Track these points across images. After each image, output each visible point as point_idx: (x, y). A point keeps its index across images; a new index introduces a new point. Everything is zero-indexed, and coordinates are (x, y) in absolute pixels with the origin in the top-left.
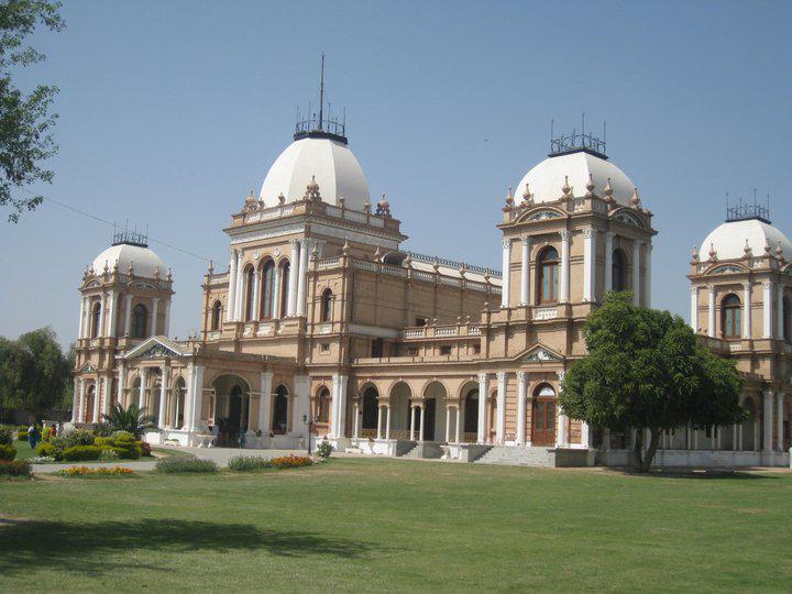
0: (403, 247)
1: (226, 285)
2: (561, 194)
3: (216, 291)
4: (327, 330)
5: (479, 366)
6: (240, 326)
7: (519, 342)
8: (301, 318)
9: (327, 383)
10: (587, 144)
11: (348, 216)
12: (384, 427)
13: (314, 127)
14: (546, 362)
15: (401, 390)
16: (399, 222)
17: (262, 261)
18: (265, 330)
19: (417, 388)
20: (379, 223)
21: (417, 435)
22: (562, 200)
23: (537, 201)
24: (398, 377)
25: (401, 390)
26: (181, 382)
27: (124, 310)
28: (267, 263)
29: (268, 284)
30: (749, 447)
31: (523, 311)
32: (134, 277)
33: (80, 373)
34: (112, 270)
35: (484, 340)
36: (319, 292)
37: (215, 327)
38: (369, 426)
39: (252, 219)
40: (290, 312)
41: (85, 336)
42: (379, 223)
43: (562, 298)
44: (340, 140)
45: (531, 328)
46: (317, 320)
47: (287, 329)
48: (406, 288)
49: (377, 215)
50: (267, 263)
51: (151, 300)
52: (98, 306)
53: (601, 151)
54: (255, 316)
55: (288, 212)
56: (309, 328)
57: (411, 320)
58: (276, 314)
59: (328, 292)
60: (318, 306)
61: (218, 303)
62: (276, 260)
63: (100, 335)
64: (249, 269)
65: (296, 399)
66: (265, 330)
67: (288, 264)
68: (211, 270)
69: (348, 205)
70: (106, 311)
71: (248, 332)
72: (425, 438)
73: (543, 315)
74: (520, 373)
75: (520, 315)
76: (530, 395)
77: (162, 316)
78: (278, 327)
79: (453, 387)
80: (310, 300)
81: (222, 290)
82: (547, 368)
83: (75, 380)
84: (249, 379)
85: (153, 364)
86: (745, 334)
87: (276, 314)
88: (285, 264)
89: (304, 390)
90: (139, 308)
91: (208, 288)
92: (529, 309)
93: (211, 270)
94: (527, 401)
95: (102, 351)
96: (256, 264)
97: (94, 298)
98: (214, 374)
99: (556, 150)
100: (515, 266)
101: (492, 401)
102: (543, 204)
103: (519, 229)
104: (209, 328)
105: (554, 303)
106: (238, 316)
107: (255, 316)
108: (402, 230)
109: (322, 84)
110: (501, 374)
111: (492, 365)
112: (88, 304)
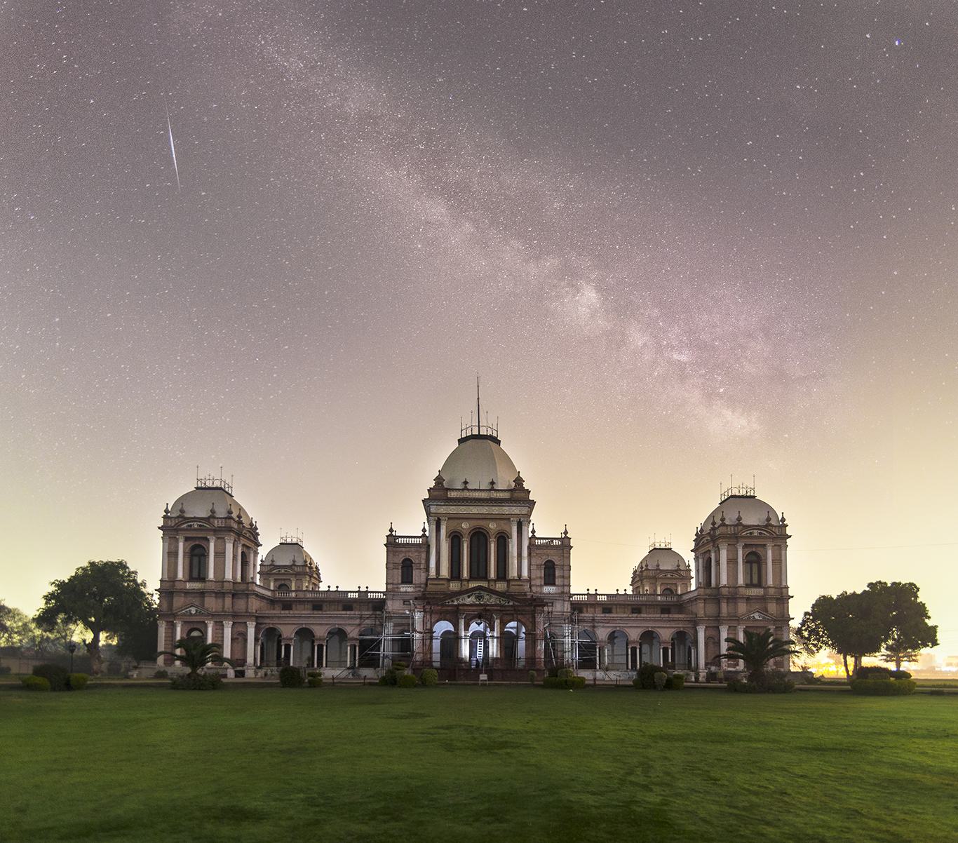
14: (761, 620)
37: (407, 579)
39: (452, 495)
47: (517, 587)
54: (465, 574)
55: (506, 495)
58: (492, 575)
62: (493, 532)
63: (211, 576)
64: (455, 539)
68: (391, 530)
71: (454, 586)
87: (492, 575)
88: (503, 540)
95: (220, 594)
100: (732, 561)
105: (759, 585)
106: (445, 572)
107: (465, 574)
109: (478, 399)
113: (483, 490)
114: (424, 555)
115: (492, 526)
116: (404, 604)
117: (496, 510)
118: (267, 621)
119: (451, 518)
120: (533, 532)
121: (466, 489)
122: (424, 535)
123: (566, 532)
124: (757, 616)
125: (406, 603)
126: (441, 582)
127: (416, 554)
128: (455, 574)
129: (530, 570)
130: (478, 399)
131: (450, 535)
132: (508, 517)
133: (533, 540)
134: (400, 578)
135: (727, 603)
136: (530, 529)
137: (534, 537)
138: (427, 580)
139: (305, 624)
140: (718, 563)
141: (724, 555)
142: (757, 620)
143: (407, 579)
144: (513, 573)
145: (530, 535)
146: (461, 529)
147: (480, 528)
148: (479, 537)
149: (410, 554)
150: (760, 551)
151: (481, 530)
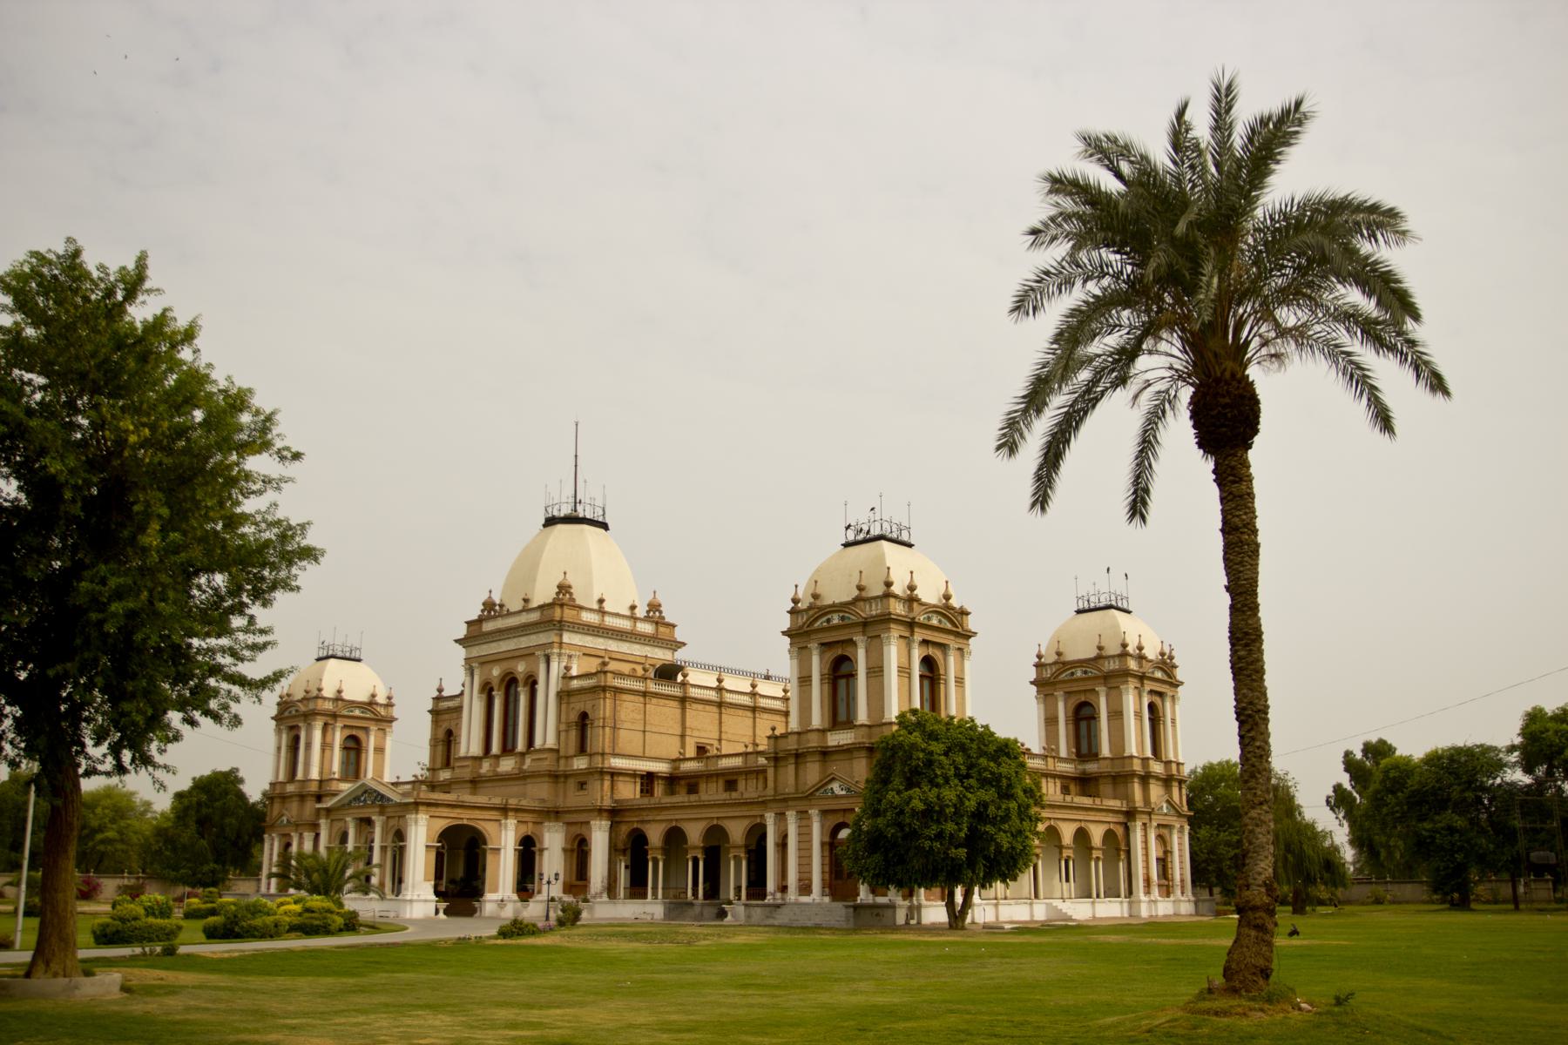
0: (680, 656)
1: (459, 709)
2: (856, 593)
4: (580, 763)
5: (764, 803)
6: (477, 760)
7: (812, 773)
8: (551, 750)
9: (583, 831)
10: (886, 531)
11: (610, 622)
12: (655, 888)
13: (566, 510)
14: (842, 797)
15: (675, 837)
16: (674, 626)
17: (502, 680)
18: (507, 765)
19: (695, 833)
20: (646, 628)
21: (695, 894)
22: (857, 600)
23: (828, 601)
25: (675, 837)
26: (400, 836)
27: (332, 747)
28: (510, 682)
29: (511, 707)
30: (1112, 892)
31: (793, 738)
32: (338, 699)
33: (272, 826)
34: (315, 693)
35: (770, 772)
36: (574, 717)
38: (638, 887)
39: (488, 626)
40: (538, 743)
41: (281, 778)
42: (646, 628)
43: (862, 716)
44: (605, 526)
45: (825, 754)
46: (572, 751)
48: (683, 709)
49: (647, 619)
50: (510, 682)
51: (366, 729)
52: (296, 739)
53: (905, 537)
54: (496, 748)
55: (534, 617)
56: (562, 762)
57: (691, 752)
59: (584, 716)
60: (573, 734)
61: (449, 733)
62: (520, 678)
63: (300, 776)
64: (487, 690)
65: (546, 853)
66: (507, 765)
67: (535, 683)
68: (440, 690)
69: (607, 607)
70: (309, 745)
71: (486, 767)
72: (706, 897)
73: (837, 739)
74: (814, 812)
75: (813, 741)
76: (827, 839)
77: (380, 750)
78: (523, 763)
79: (737, 831)
80: (563, 727)
82: (844, 804)
83: (266, 836)
84: (488, 828)
85: (364, 813)
86: (1105, 751)
88: (532, 683)
89: (553, 841)
90: (352, 744)
91: (435, 713)
92: (823, 731)
93: (440, 690)
94: (823, 844)
96: (495, 683)
97: (292, 728)
98: (441, 825)
99: (851, 536)
100: (804, 680)
101: (782, 845)
102: (834, 605)
103: (808, 634)
104: (438, 765)
106: (476, 749)
107: (496, 748)
108: (679, 635)
110: (791, 816)
111: (781, 802)
112: (284, 736)
115: (521, 668)
122: (462, 693)
124: (836, 786)
129: (559, 733)
135: (796, 764)
142: (837, 797)
143: (447, 764)
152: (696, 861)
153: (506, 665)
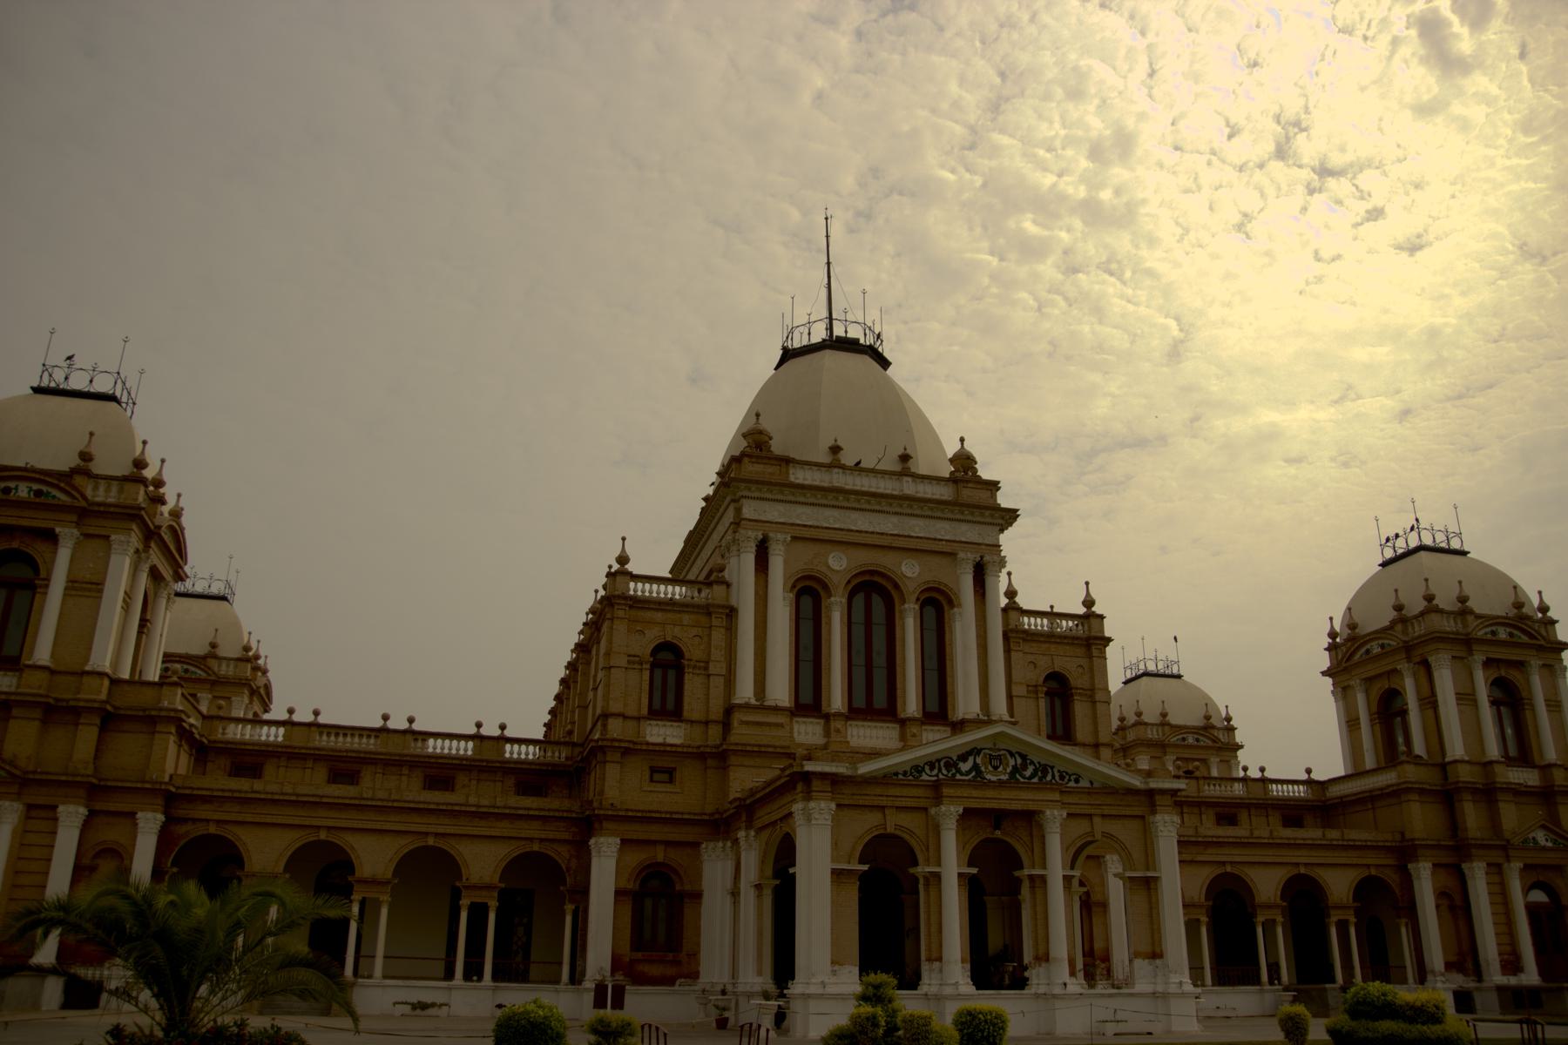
3: (659, 616)
14: (1544, 848)
24: (1224, 863)
39: (799, 476)
54: (836, 699)
58: (911, 704)
62: (911, 590)
64: (809, 592)
68: (623, 559)
70: (87, 588)
71: (807, 732)
81: (686, 619)
87: (911, 704)
88: (937, 604)
93: (623, 559)
100: (1466, 698)
106: (780, 691)
107: (836, 699)
109: (828, 263)
113: (884, 473)
114: (718, 636)
115: (910, 571)
116: (652, 780)
117: (918, 528)
118: (202, 811)
119: (802, 537)
120: (1011, 594)
121: (836, 465)
123: (1089, 602)
125: (656, 776)
126: (772, 719)
127: (695, 631)
128: (809, 704)
129: (1010, 697)
130: (828, 263)
131: (794, 586)
132: (947, 549)
133: (1013, 614)
134: (645, 701)
136: (1003, 587)
137: (1012, 608)
138: (729, 710)
139: (329, 828)
140: (1430, 702)
141: (1445, 682)
144: (966, 703)
145: (1004, 601)
146: (824, 569)
147: (872, 573)
148: (873, 589)
149: (677, 629)
150: (1514, 675)
151: (877, 579)
152: (1343, 926)
153: (866, 559)
